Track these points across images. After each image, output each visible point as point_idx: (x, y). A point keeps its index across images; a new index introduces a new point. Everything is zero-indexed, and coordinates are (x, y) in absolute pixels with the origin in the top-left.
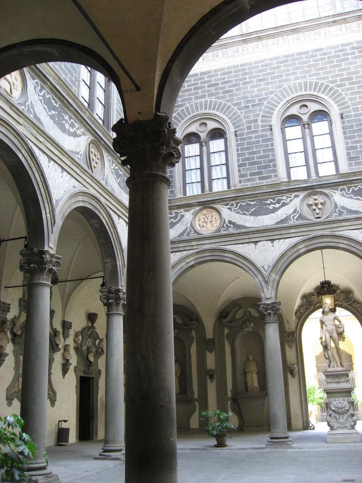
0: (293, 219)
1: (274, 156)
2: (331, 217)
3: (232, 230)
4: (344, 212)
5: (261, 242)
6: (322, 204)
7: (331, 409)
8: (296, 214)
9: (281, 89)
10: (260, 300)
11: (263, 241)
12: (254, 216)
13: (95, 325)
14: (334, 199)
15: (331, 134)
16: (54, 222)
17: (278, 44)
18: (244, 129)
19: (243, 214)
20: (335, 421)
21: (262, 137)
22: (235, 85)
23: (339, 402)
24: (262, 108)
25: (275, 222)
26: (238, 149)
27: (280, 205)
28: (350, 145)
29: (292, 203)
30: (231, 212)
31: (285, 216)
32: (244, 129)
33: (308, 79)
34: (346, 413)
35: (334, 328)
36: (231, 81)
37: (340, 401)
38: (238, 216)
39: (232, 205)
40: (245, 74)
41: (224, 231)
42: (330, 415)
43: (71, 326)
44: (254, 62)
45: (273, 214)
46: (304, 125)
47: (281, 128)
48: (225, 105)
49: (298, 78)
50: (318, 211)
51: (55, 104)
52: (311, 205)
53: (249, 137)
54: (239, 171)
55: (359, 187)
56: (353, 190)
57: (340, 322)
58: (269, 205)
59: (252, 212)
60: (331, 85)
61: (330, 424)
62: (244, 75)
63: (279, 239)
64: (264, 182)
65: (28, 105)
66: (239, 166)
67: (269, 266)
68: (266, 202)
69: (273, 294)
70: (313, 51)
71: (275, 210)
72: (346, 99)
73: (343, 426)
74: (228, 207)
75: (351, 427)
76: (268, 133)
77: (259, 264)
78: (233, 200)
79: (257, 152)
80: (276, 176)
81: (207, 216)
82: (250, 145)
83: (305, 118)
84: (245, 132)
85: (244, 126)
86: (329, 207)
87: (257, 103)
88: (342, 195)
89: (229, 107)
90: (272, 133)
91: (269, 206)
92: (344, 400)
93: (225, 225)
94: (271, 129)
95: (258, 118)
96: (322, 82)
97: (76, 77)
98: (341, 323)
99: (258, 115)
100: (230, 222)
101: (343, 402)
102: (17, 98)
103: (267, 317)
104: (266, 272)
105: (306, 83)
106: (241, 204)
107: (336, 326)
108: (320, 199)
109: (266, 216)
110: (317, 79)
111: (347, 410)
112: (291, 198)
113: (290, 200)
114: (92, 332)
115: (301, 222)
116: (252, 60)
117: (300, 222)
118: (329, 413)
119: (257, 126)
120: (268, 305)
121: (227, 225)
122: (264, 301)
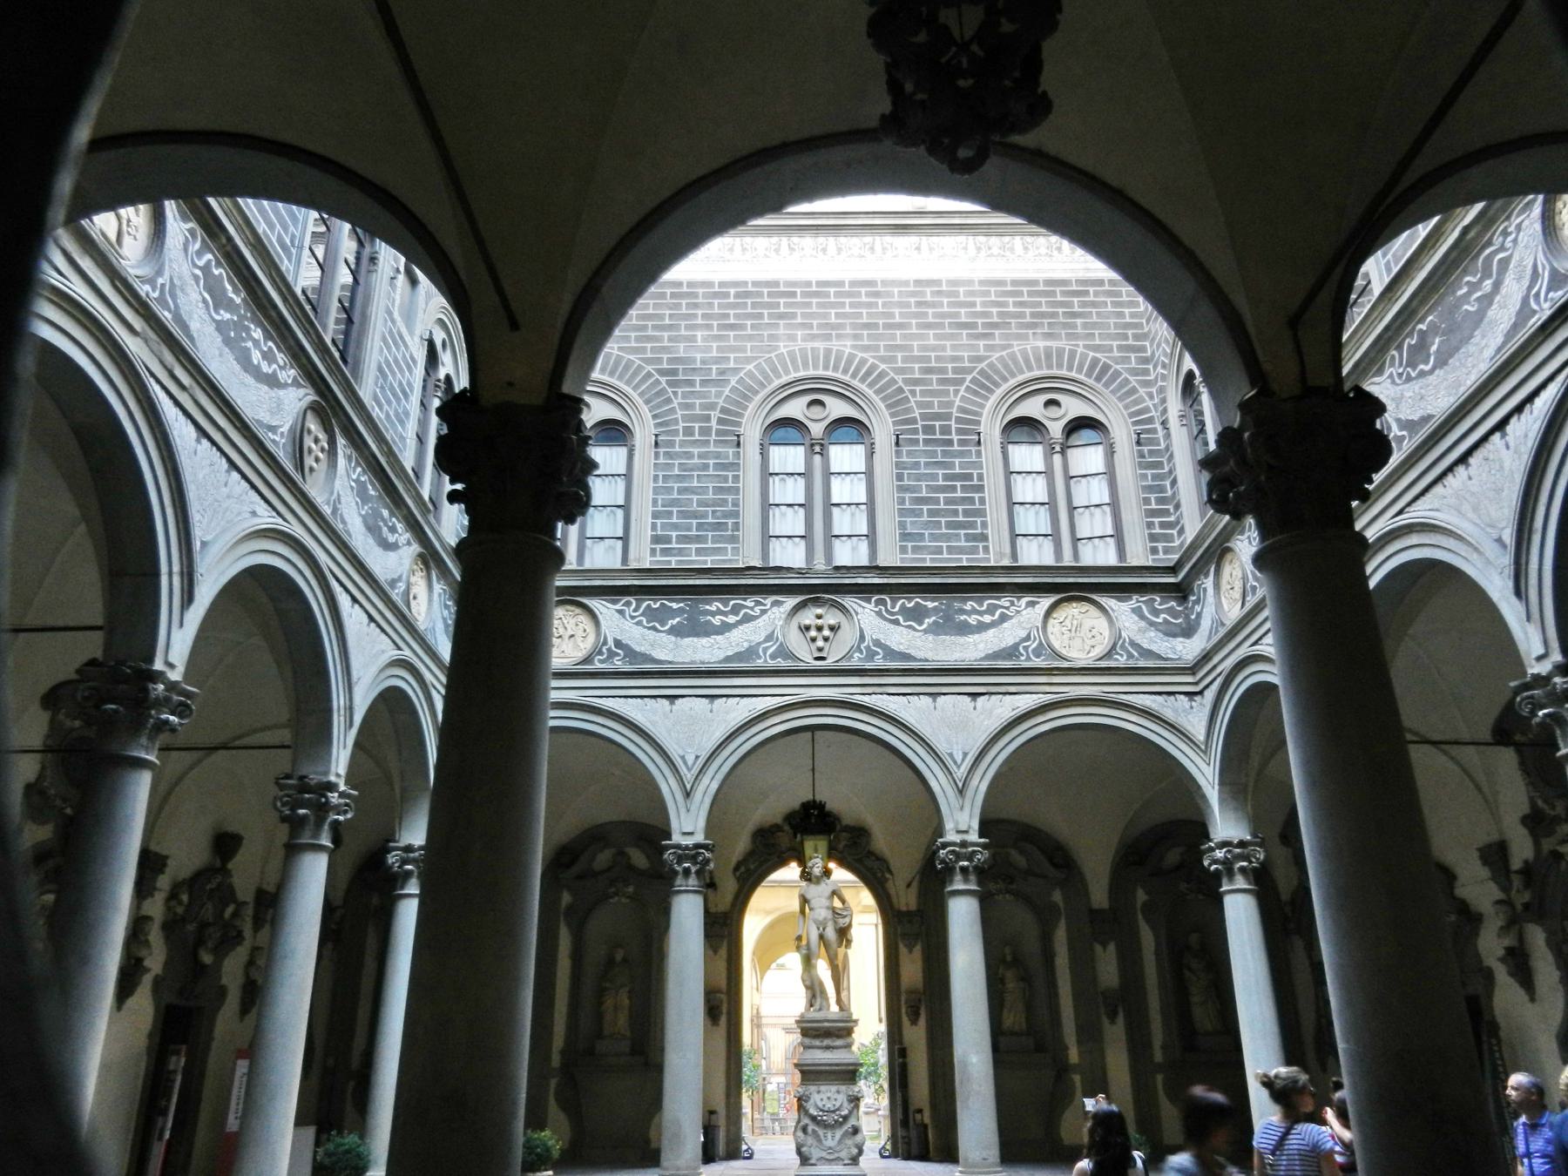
0: (765, 654)
1: (738, 505)
2: (850, 661)
3: (620, 663)
4: (878, 654)
5: (684, 699)
6: (832, 628)
7: (807, 1112)
8: (771, 643)
9: (773, 355)
10: (668, 836)
11: (690, 696)
12: (676, 636)
13: (230, 866)
14: (859, 620)
15: (869, 474)
16: (188, 598)
17: (777, 251)
18: (676, 432)
19: (649, 628)
20: (815, 1143)
21: (717, 458)
22: (670, 327)
23: (827, 1097)
24: (723, 392)
25: (722, 656)
26: (658, 476)
27: (738, 619)
28: (907, 506)
29: (765, 617)
30: (623, 620)
31: (746, 645)
32: (676, 432)
33: (835, 345)
34: (841, 1124)
35: (829, 914)
36: (661, 317)
37: (829, 1095)
38: (638, 631)
39: (628, 604)
40: (696, 306)
41: (601, 662)
42: (804, 1130)
43: (165, 865)
44: (720, 283)
45: (719, 638)
46: (812, 445)
47: (761, 444)
48: (640, 368)
49: (813, 337)
50: (820, 643)
51: (233, 296)
52: (808, 628)
53: (686, 452)
54: (654, 527)
55: (917, 603)
56: (903, 606)
57: (843, 902)
58: (713, 614)
59: (672, 626)
60: (883, 366)
61: (803, 1149)
62: (693, 309)
63: (728, 696)
64: (709, 562)
65: (163, 285)
66: (655, 515)
67: (697, 757)
68: (708, 607)
69: (702, 823)
70: (853, 283)
71: (725, 628)
72: (909, 401)
73: (832, 1157)
74: (618, 607)
75: (851, 1159)
76: (731, 451)
77: (674, 751)
78: (630, 594)
79: (699, 490)
80: (736, 550)
81: (565, 622)
82: (685, 471)
83: (817, 430)
84: (681, 438)
85: (677, 424)
86: (847, 637)
87: (714, 377)
88: (879, 614)
89: (649, 375)
90: (739, 452)
91: (713, 617)
92: (838, 1092)
93: (604, 650)
94: (738, 445)
95: (712, 413)
96: (864, 355)
97: (293, 237)
98: (846, 905)
99: (712, 406)
100: (618, 643)
101: (836, 1096)
102: (133, 262)
103: (679, 877)
104: (689, 770)
105: (828, 352)
106: (649, 606)
107: (833, 910)
108: (832, 618)
109: (704, 641)
110: (853, 347)
111: (846, 1118)
112: (765, 605)
113: (761, 610)
114: (219, 885)
115: (782, 663)
116: (716, 277)
117: (779, 662)
118: (802, 1124)
119: (705, 431)
120: (687, 848)
121: (609, 650)
122: (677, 838)
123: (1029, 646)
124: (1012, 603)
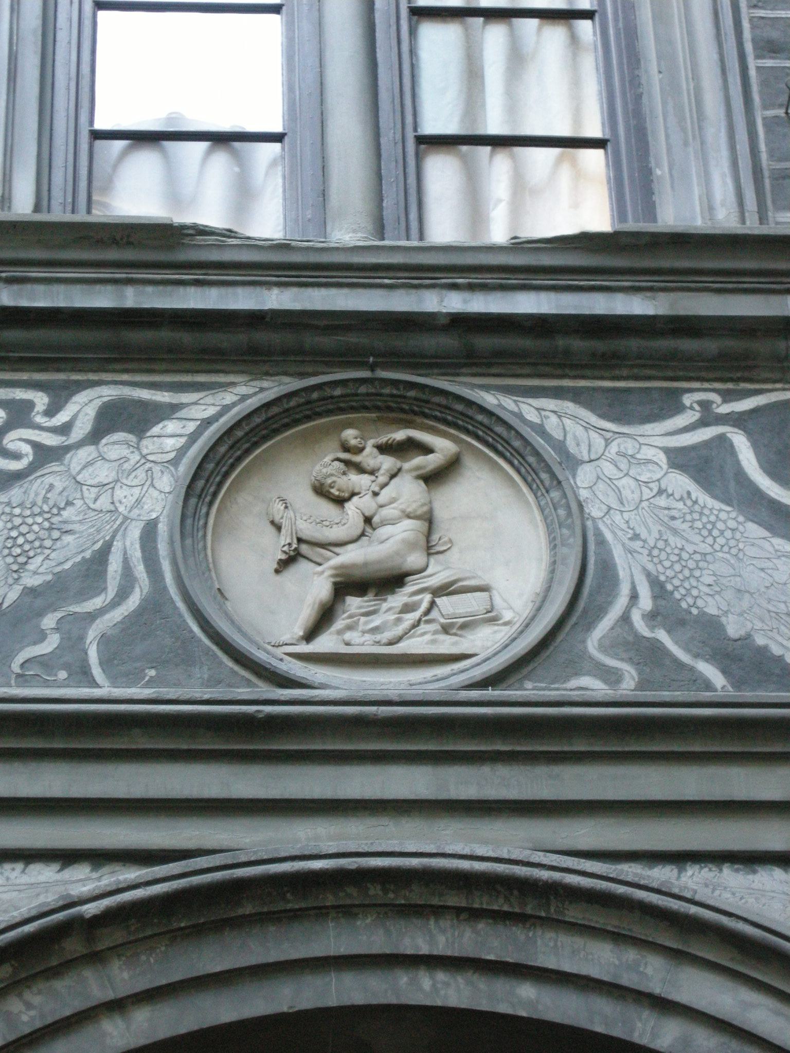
123: (92, 617)
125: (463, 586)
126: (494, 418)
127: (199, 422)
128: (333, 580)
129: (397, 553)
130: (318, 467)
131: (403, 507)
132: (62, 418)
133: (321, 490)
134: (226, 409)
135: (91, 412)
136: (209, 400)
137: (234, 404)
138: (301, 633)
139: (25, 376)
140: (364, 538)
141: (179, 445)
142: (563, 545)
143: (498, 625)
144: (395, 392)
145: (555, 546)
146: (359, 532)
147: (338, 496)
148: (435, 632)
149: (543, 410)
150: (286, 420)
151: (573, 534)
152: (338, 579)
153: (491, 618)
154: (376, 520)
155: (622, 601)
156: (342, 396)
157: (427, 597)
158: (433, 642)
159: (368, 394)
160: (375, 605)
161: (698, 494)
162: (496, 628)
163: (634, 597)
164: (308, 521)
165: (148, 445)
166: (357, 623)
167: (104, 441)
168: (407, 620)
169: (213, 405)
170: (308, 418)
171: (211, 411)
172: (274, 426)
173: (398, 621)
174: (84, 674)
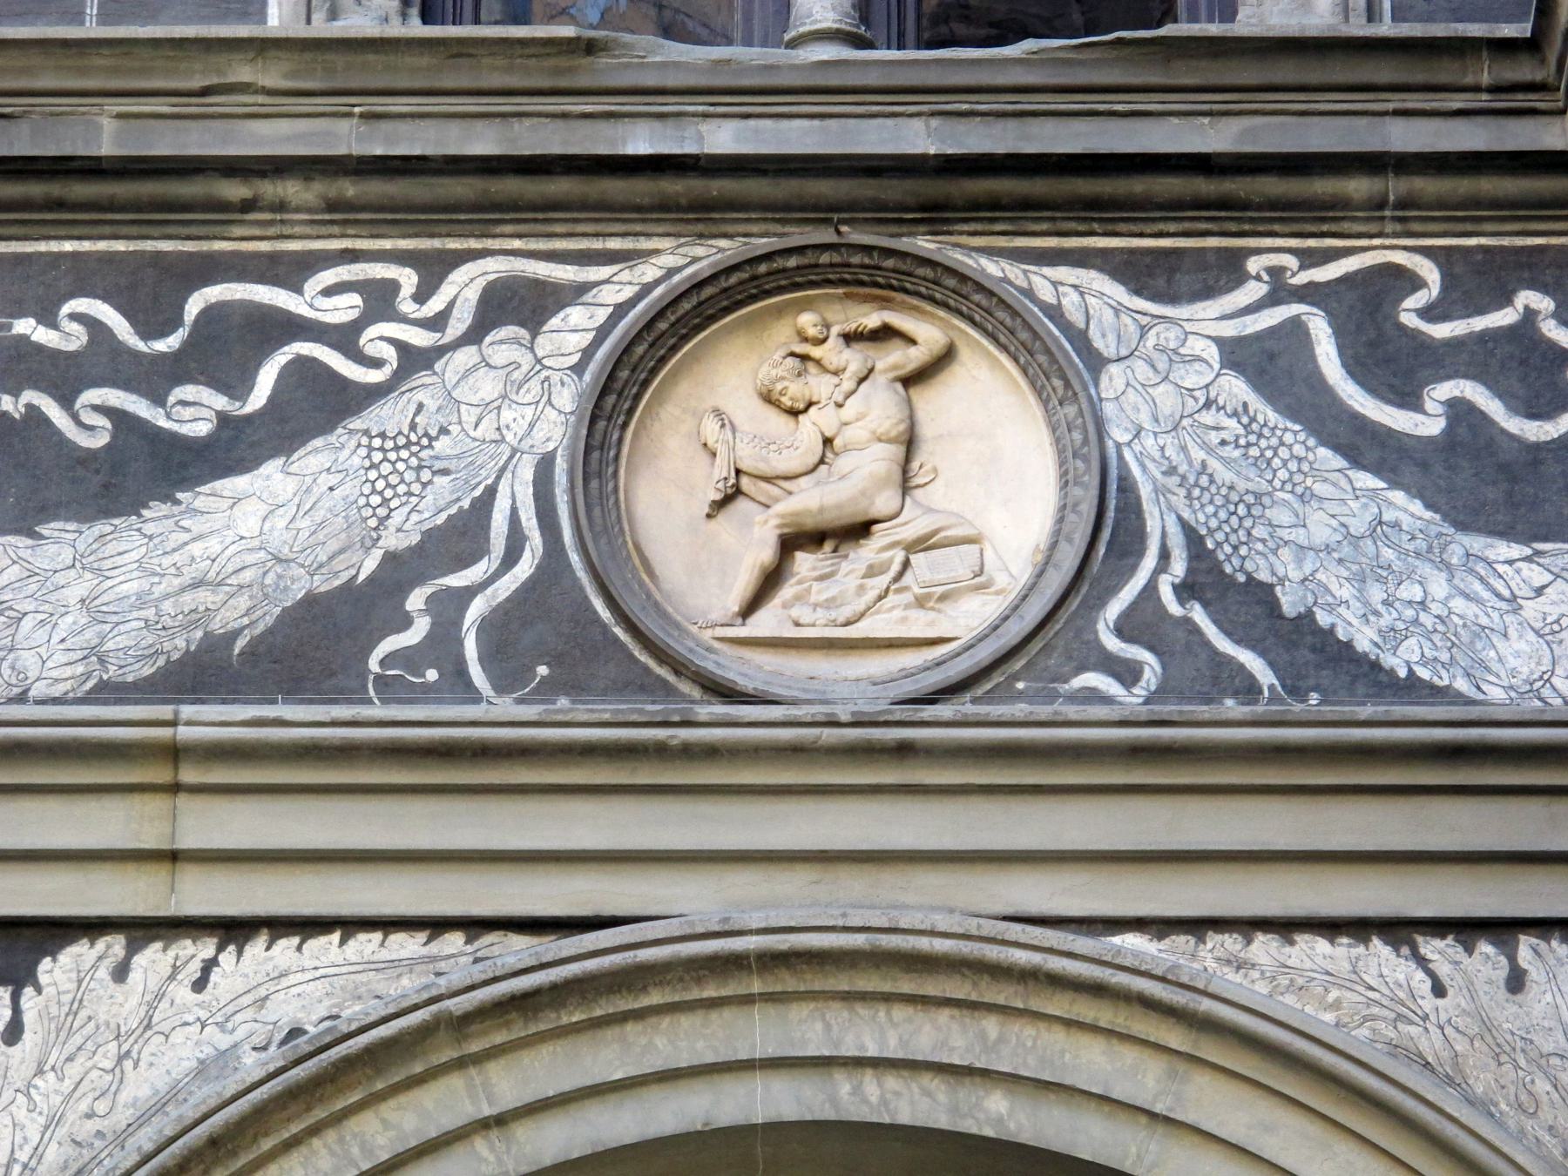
124: (380, 300)
125: (945, 537)
126: (995, 300)
127: (611, 309)
128: (778, 532)
129: (863, 493)
130: (764, 369)
131: (873, 426)
132: (435, 305)
133: (768, 398)
134: (647, 289)
135: (472, 295)
136: (625, 276)
137: (657, 282)
138: (736, 609)
139: (387, 244)
140: (823, 468)
141: (585, 343)
142: (1076, 484)
143: (988, 594)
144: (867, 261)
145: (1067, 482)
146: (816, 459)
147: (792, 408)
148: (907, 607)
149: (1062, 284)
150: (725, 303)
151: (1088, 470)
152: (786, 530)
153: (980, 582)
154: (837, 443)
155: (1149, 562)
156: (798, 268)
157: (899, 556)
158: (904, 620)
159: (832, 265)
160: (832, 565)
161: (1257, 403)
162: (985, 597)
163: (1165, 555)
164: (751, 444)
165: (544, 344)
166: (808, 591)
167: (488, 339)
168: (872, 588)
169: (630, 283)
170: (754, 298)
171: (628, 292)
172: (710, 312)
173: (861, 589)
174: (458, 683)
